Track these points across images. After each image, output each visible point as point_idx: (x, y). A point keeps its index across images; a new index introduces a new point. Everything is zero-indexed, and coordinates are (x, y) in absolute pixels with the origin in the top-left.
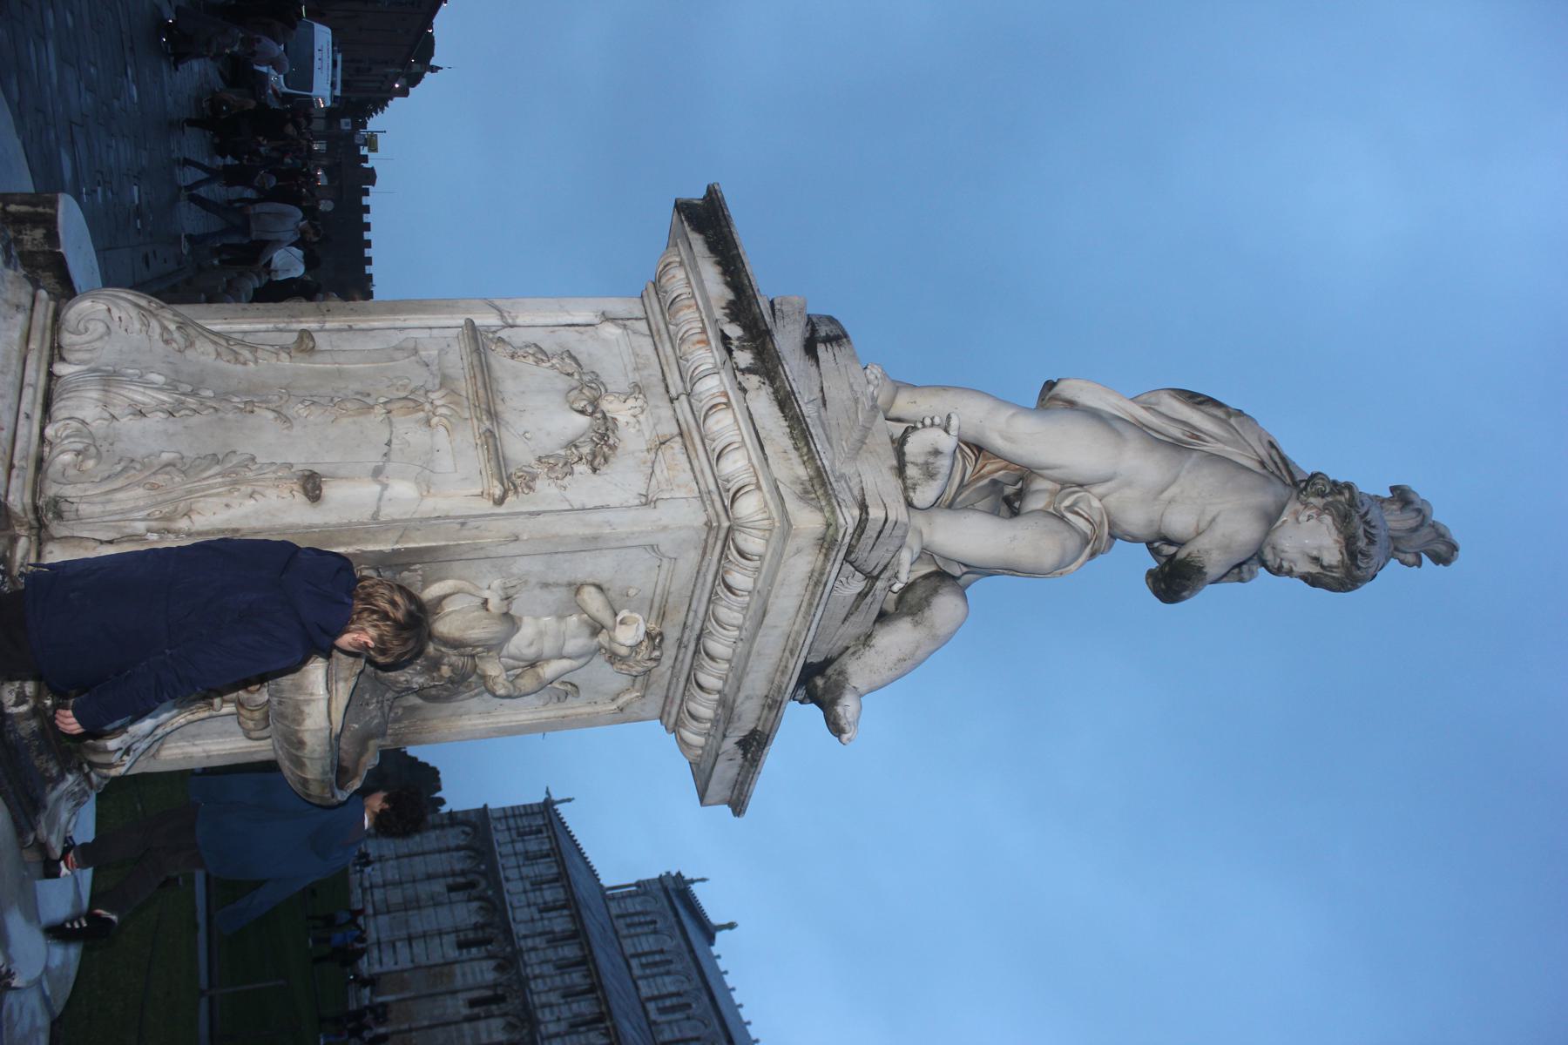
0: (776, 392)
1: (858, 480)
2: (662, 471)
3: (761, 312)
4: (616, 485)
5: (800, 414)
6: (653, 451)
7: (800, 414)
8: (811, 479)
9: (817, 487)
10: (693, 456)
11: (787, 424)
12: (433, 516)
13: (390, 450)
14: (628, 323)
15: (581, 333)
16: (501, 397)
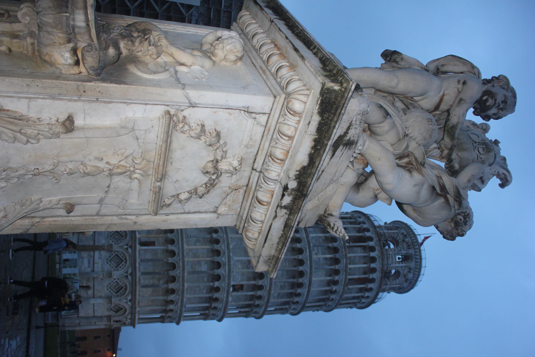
0: (288, 219)
1: (304, 216)
2: (230, 201)
3: (311, 184)
4: (207, 202)
5: (288, 236)
6: (231, 190)
7: (288, 236)
8: (274, 256)
9: (274, 260)
10: (246, 198)
11: (282, 233)
12: (123, 214)
13: (109, 190)
14: (257, 116)
15: (230, 114)
16: (171, 162)
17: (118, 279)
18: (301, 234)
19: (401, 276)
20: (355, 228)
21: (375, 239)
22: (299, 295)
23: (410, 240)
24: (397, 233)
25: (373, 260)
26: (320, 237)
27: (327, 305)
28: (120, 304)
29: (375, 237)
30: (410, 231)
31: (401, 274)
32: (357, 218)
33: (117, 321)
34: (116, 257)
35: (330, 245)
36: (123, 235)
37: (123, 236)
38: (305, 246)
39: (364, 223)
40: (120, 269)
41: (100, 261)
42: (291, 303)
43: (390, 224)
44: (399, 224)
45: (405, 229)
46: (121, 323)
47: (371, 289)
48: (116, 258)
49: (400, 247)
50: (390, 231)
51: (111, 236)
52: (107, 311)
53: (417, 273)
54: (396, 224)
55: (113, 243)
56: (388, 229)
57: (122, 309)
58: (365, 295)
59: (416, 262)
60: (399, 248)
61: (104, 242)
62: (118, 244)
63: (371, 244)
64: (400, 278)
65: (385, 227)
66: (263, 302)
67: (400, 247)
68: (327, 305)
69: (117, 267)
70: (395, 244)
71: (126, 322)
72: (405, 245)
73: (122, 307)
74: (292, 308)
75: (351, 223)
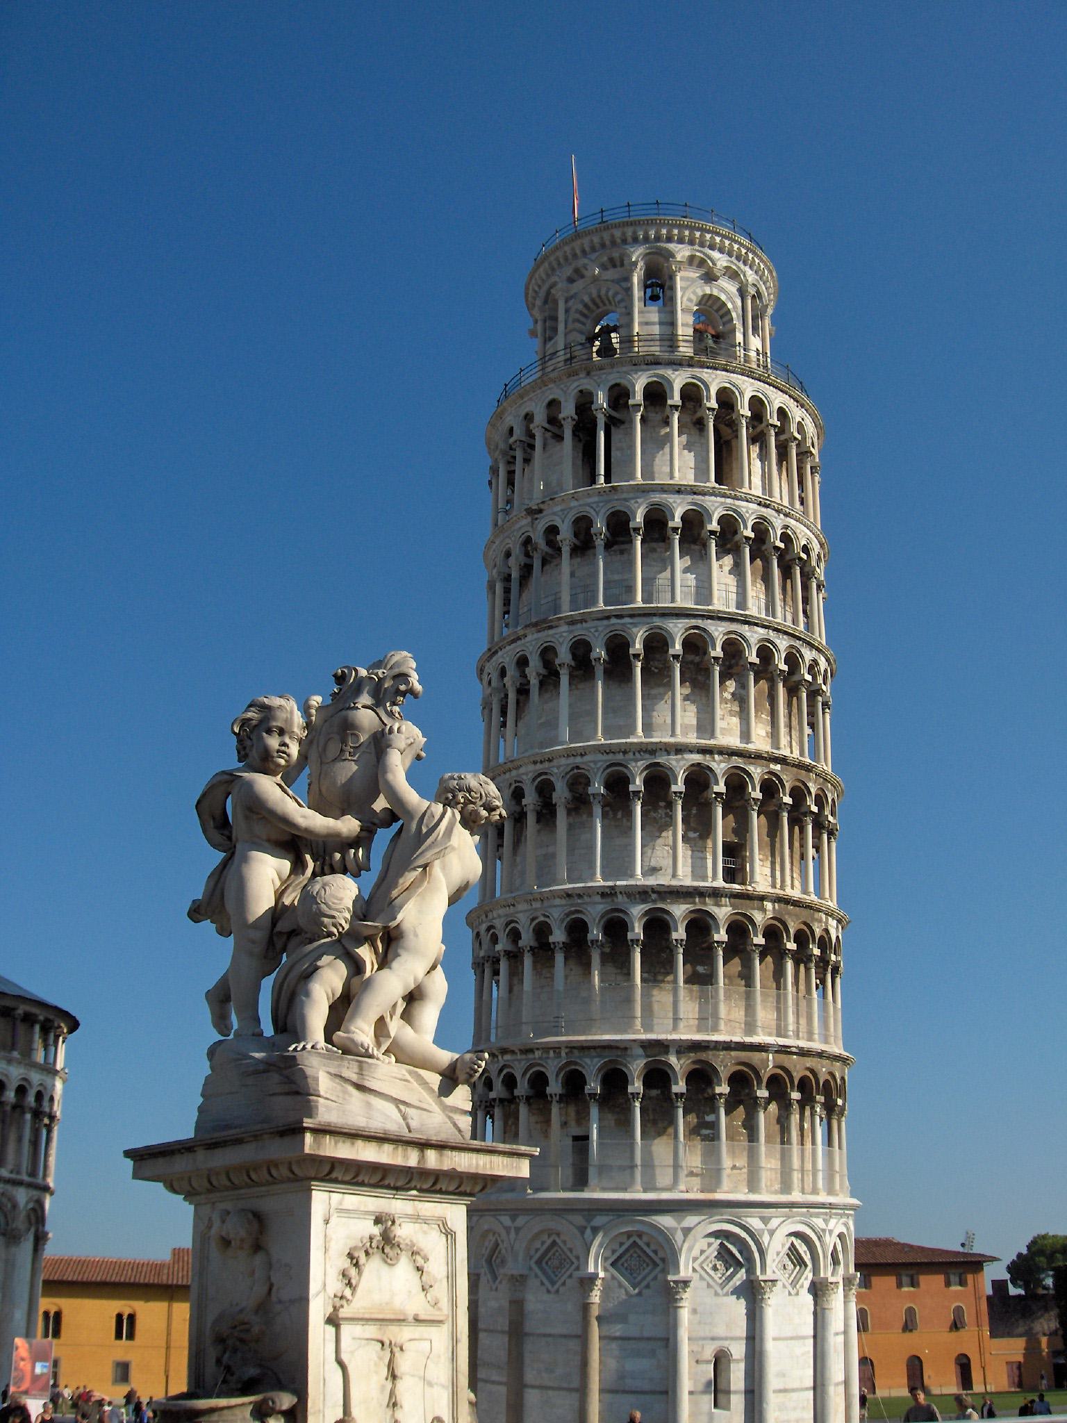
17: (695, 1259)
18: (561, 640)
19: (715, 292)
20: (545, 446)
21: (585, 383)
22: (765, 653)
23: (593, 256)
24: (566, 301)
25: (656, 394)
26: (572, 574)
27: (804, 556)
28: (778, 1254)
29: (576, 384)
30: (559, 254)
31: (708, 291)
32: (511, 440)
33: (836, 1262)
34: (623, 1265)
35: (599, 542)
36: (549, 1242)
37: (554, 1243)
38: (600, 629)
39: (529, 417)
40: (661, 1254)
41: (632, 1318)
42: (796, 678)
43: (536, 322)
44: (537, 289)
45: (553, 270)
46: (839, 1248)
47: (757, 404)
48: (626, 1265)
49: (616, 294)
50: (561, 327)
51: (553, 1283)
52: (797, 1294)
53: (708, 236)
54: (534, 298)
55: (577, 1274)
56: (555, 330)
57: (793, 1247)
58: (775, 426)
59: (669, 239)
60: (619, 297)
61: (570, 1307)
62: (578, 1258)
63: (601, 399)
64: (723, 297)
65: (547, 340)
66: (784, 777)
67: (616, 294)
68: (804, 556)
69: (656, 1265)
70: (605, 308)
71: (836, 1232)
72: (611, 274)
73: (788, 1245)
74: (808, 678)
75: (527, 461)
